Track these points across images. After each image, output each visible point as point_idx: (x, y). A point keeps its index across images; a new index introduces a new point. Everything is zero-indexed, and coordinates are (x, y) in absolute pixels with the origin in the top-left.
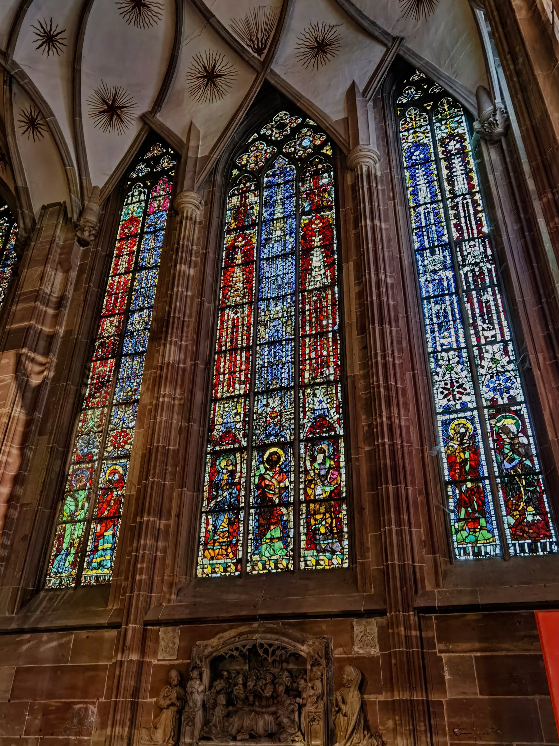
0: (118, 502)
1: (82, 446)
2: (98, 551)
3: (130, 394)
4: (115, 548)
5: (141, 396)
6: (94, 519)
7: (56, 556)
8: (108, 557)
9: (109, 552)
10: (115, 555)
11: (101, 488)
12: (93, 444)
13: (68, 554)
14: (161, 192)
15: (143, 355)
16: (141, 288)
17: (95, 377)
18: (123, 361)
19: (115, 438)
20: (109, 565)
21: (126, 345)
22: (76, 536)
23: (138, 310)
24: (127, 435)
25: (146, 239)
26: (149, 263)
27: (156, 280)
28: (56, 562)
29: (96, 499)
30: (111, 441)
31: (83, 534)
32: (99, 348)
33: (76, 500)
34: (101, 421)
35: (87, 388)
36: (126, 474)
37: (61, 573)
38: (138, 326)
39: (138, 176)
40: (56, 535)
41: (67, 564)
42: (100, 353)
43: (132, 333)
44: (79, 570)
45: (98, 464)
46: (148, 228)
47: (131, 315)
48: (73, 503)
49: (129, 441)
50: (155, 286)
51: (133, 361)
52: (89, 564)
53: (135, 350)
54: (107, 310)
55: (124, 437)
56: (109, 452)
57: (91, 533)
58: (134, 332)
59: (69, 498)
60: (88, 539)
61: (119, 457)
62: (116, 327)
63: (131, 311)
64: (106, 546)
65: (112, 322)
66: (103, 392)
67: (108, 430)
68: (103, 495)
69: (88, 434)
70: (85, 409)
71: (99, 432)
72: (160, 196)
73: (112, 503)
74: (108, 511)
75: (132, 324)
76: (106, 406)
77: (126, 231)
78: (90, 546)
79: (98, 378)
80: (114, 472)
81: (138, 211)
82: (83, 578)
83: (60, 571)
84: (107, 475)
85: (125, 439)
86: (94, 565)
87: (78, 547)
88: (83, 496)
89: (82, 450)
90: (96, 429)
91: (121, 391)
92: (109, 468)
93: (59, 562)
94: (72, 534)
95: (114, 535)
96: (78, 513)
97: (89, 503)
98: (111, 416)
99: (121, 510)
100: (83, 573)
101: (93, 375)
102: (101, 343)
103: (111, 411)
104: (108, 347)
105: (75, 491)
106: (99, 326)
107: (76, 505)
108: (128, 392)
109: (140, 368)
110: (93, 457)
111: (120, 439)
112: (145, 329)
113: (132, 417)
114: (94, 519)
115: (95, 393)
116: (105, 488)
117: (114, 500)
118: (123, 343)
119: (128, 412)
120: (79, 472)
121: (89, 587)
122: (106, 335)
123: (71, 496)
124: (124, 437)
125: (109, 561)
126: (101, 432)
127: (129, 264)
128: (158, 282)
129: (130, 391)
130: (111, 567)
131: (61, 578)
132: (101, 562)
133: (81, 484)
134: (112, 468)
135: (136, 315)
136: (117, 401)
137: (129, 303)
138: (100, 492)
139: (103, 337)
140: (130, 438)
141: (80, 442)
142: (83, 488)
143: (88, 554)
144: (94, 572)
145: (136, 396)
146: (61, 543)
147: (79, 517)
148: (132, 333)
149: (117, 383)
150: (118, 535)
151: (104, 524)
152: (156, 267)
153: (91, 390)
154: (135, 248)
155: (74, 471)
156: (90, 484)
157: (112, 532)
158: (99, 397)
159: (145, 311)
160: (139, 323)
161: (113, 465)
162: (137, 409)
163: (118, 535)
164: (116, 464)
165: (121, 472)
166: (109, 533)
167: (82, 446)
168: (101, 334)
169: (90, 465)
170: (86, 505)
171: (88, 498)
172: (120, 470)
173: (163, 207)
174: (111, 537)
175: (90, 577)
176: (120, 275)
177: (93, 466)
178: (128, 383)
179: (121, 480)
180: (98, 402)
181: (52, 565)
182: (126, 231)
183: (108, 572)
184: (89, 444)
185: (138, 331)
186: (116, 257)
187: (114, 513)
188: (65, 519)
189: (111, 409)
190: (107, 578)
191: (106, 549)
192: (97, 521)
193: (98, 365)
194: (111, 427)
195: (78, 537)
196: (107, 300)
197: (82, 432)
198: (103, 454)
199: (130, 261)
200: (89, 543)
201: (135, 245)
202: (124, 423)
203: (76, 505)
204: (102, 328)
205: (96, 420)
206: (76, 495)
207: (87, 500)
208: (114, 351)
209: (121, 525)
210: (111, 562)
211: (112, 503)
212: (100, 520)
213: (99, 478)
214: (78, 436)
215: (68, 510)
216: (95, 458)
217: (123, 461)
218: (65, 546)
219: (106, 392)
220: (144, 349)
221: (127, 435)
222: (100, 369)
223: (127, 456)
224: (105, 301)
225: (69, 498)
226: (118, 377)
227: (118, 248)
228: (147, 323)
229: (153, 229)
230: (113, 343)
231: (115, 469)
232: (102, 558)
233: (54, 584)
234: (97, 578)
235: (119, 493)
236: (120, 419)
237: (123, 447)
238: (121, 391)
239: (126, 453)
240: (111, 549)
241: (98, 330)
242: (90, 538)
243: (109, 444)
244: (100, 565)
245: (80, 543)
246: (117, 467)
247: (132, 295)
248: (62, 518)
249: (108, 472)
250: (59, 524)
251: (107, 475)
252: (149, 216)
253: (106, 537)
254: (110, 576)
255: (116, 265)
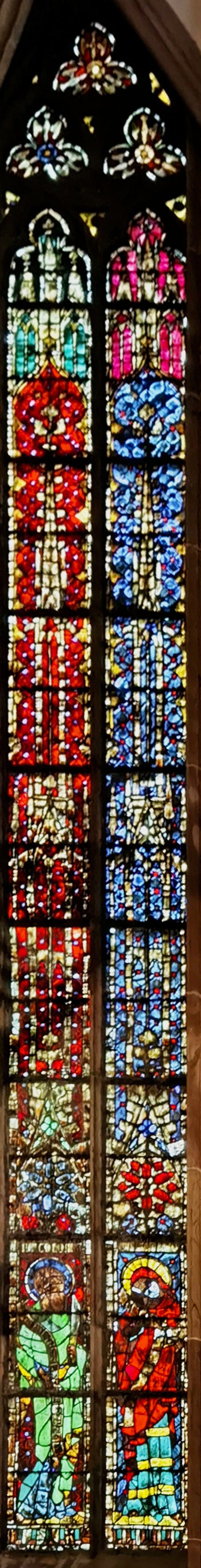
0: (170, 1354)
1: (32, 1190)
2: (137, 1472)
3: (154, 1053)
4: (182, 1470)
5: (192, 1065)
6: (110, 1393)
7: (22, 1475)
8: (169, 1489)
9: (168, 1477)
10: (184, 1486)
11: (115, 1316)
12: (67, 1186)
13: (55, 1473)
14: (149, 287)
15: (176, 935)
16: (133, 688)
17: (32, 977)
18: (114, 941)
19: (132, 1177)
20: (174, 1507)
21: (115, 887)
22: (66, 1430)
23: (133, 770)
24: (167, 1177)
25: (122, 489)
26: (146, 593)
27: (182, 671)
28: (24, 1491)
29: (106, 1342)
30: (122, 1188)
31: (87, 1427)
32: (22, 879)
33: (46, 1337)
34: (78, 1121)
35: (9, 1010)
36: (180, 1285)
37: (47, 1516)
38: (144, 831)
39: (44, 174)
40: (8, 1424)
41: (57, 1497)
42: (30, 899)
43: (130, 851)
44: (93, 1511)
45: (94, 1248)
46: (120, 438)
47: (115, 782)
48: (41, 1346)
49: (176, 1196)
50: (179, 692)
51: (147, 949)
52: (121, 1500)
53: (147, 912)
54: (26, 746)
55: (158, 1181)
56: (121, 1219)
57: (108, 1427)
58: (137, 846)
59: (24, 1330)
60: (103, 1444)
61: (152, 1237)
62: (70, 816)
63: (110, 769)
64: (156, 1462)
65: (51, 794)
66: (67, 1033)
67: (104, 1154)
68: (126, 1333)
69: (45, 1154)
70: (18, 1078)
71: (77, 1156)
72: (146, 305)
73: (155, 1357)
74: (148, 1376)
75: (122, 817)
76: (87, 1080)
77: (39, 429)
78: (112, 1459)
79: (42, 983)
80: (145, 1276)
81: (69, 349)
82: (108, 1533)
83: (43, 1511)
84: (127, 1283)
85: (164, 1187)
86: (134, 1504)
87: (80, 1457)
88: (67, 1331)
89: (36, 1201)
90: (66, 1145)
91: (123, 1038)
92: (127, 1262)
93: (35, 1489)
94: (55, 1426)
95: (175, 1439)
96: (61, 1373)
97: (87, 1349)
98: (106, 1113)
99: (184, 1378)
100: (108, 1521)
101: (22, 972)
102: (28, 864)
103: (105, 1100)
104: (55, 882)
105: (39, 1313)
106: (11, 800)
107: (52, 1352)
108: (146, 1048)
109: (173, 975)
110: (73, 1225)
111: (147, 1186)
112: (170, 845)
113: (171, 1127)
114: (110, 1393)
115: (42, 1032)
116: (124, 1317)
117: (160, 1350)
118: (104, 881)
119: (160, 1110)
120: (39, 1263)
121: (126, 1553)
122: (42, 839)
123: (30, 1326)
124: (158, 1181)
125: (172, 1499)
126: (83, 1155)
127: (72, 576)
128: (189, 678)
129: (155, 1044)
130: (180, 1512)
131: (48, 1528)
132: (150, 1498)
133: (54, 1296)
134: (136, 1265)
135: (132, 788)
136: (118, 1071)
137: (100, 738)
138: (115, 1326)
139: (31, 845)
140: (174, 1188)
141: (25, 1176)
142: (64, 1308)
143: (110, 1476)
144: (136, 1520)
145: (174, 1065)
146: (28, 1445)
147: (65, 1384)
148: (130, 851)
149: (106, 1012)
150: (185, 1437)
151: (142, 1409)
152: (170, 615)
153: (25, 1020)
154: (84, 516)
155: (26, 1259)
156: (81, 1301)
157: (167, 1431)
158: (55, 1047)
159: (160, 779)
160: (144, 817)
161: (138, 1256)
162: (184, 1105)
163: (185, 1437)
164: (146, 1255)
165: (167, 1279)
166: (160, 1432)
167: (32, 1190)
168: (23, 830)
169: (70, 1247)
170: (81, 1355)
171: (82, 1337)
172: (163, 1272)
173: (166, 362)
174: (166, 1443)
175: (129, 1531)
176: (48, 613)
177: (78, 1253)
178: (142, 1017)
179: (169, 1299)
180: (58, 1062)
181: (17, 1494)
182: (39, 429)
183: (174, 1523)
184: (54, 1187)
185: (148, 846)
186: (20, 534)
187: (166, 1385)
188: (24, 1384)
189: (104, 1092)
190: (173, 1536)
191: (160, 1470)
192: (122, 1400)
193: (32, 940)
194: (111, 1146)
195: (73, 1434)
196: (19, 707)
197: (25, 1148)
198: (104, 1223)
199: (74, 568)
200: (109, 1452)
201: (81, 502)
202: (149, 1141)
203: (52, 1352)
204: (23, 809)
205: (61, 1116)
206: (45, 1324)
207: (80, 1342)
208: (78, 900)
209: (191, 1415)
210: (179, 1500)
211: (155, 1357)
212: (129, 1398)
213: (104, 1286)
214: (14, 1157)
215: (30, 1364)
216: (81, 1229)
217: (166, 1248)
218: (41, 1452)
219: (77, 1034)
220: (175, 915)
221: (167, 1177)
222: (42, 955)
223: (175, 1237)
224: (11, 706)
225: (24, 1330)
226: (106, 994)
227: (18, 497)
228: (172, 826)
229: (138, 453)
230: (71, 873)
231: (147, 1269)
232: (153, 1491)
233: (31, 1540)
234: (148, 1535)
235: (170, 1333)
236: (136, 1126)
237: (160, 1209)
238: (123, 1038)
239: (171, 1228)
240: (171, 1470)
241: (9, 814)
242: (109, 1438)
243: (117, 1196)
244: (150, 1506)
245: (82, 1448)
246: (152, 1264)
247: (105, 709)
248: (17, 1382)
249: (128, 1273)
250: (11, 1396)
251: (127, 1283)
252: (115, 387)
253: (153, 1442)
254: (182, 1533)
255: (26, 567)
